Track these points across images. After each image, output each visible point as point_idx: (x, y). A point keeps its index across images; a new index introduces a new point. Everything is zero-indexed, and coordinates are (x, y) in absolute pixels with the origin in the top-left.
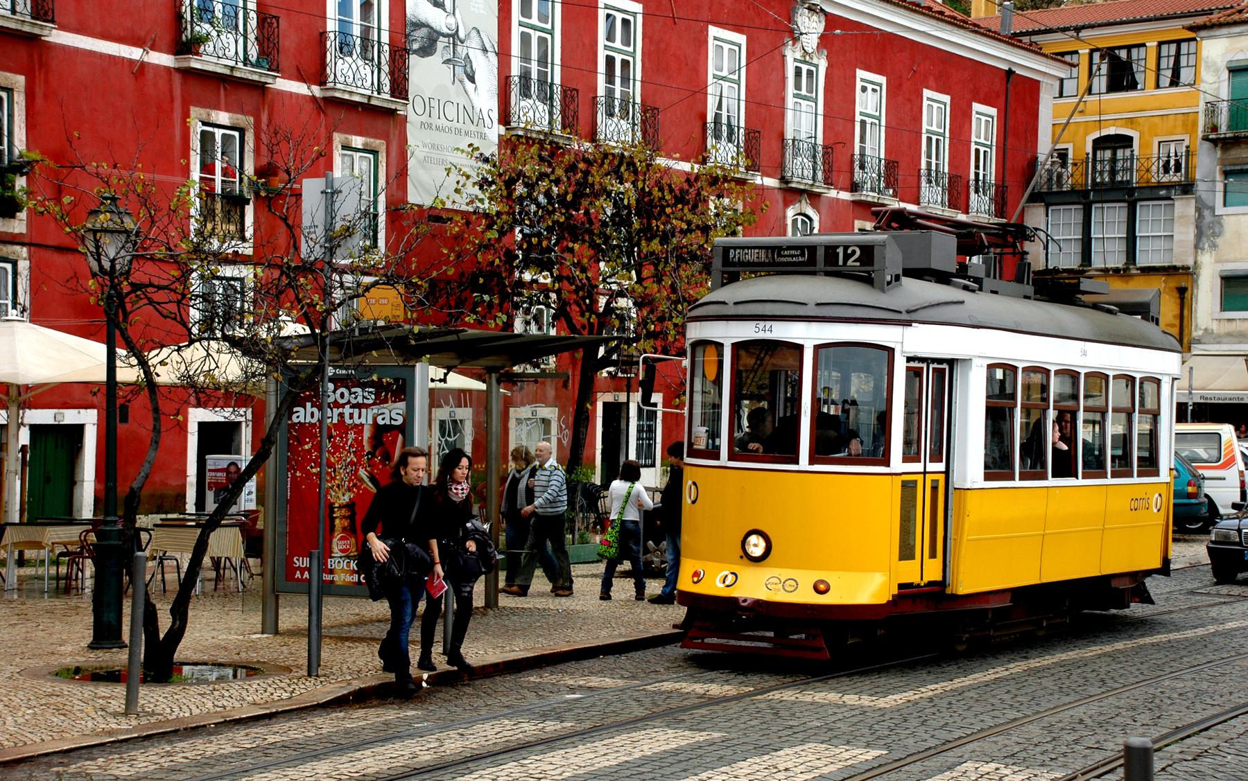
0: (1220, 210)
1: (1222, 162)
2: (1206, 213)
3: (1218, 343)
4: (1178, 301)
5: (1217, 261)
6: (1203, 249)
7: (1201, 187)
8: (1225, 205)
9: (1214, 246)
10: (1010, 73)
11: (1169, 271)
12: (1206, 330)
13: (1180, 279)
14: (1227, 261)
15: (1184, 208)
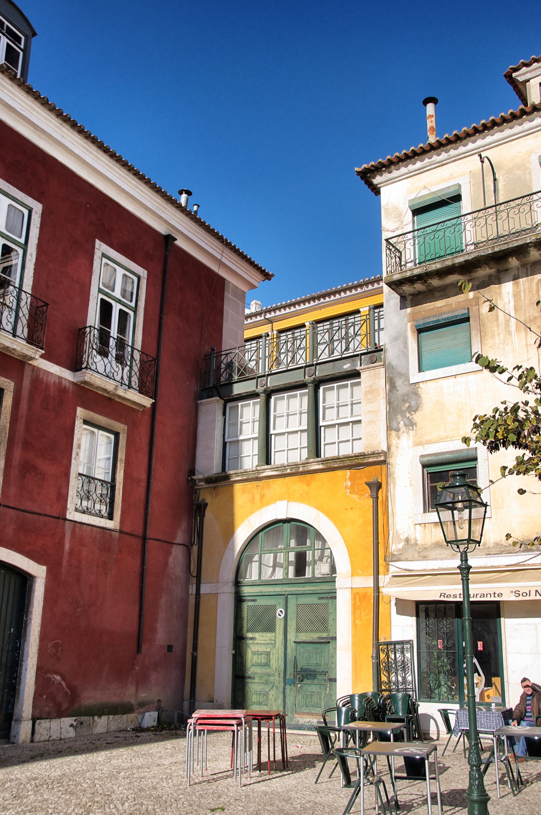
0: (415, 377)
1: (413, 318)
2: (399, 383)
3: (425, 558)
4: (370, 501)
5: (417, 444)
6: (398, 430)
7: (391, 354)
8: (420, 370)
9: (411, 424)
10: (169, 239)
11: (355, 463)
12: (407, 540)
13: (370, 470)
14: (429, 442)
15: (373, 379)
